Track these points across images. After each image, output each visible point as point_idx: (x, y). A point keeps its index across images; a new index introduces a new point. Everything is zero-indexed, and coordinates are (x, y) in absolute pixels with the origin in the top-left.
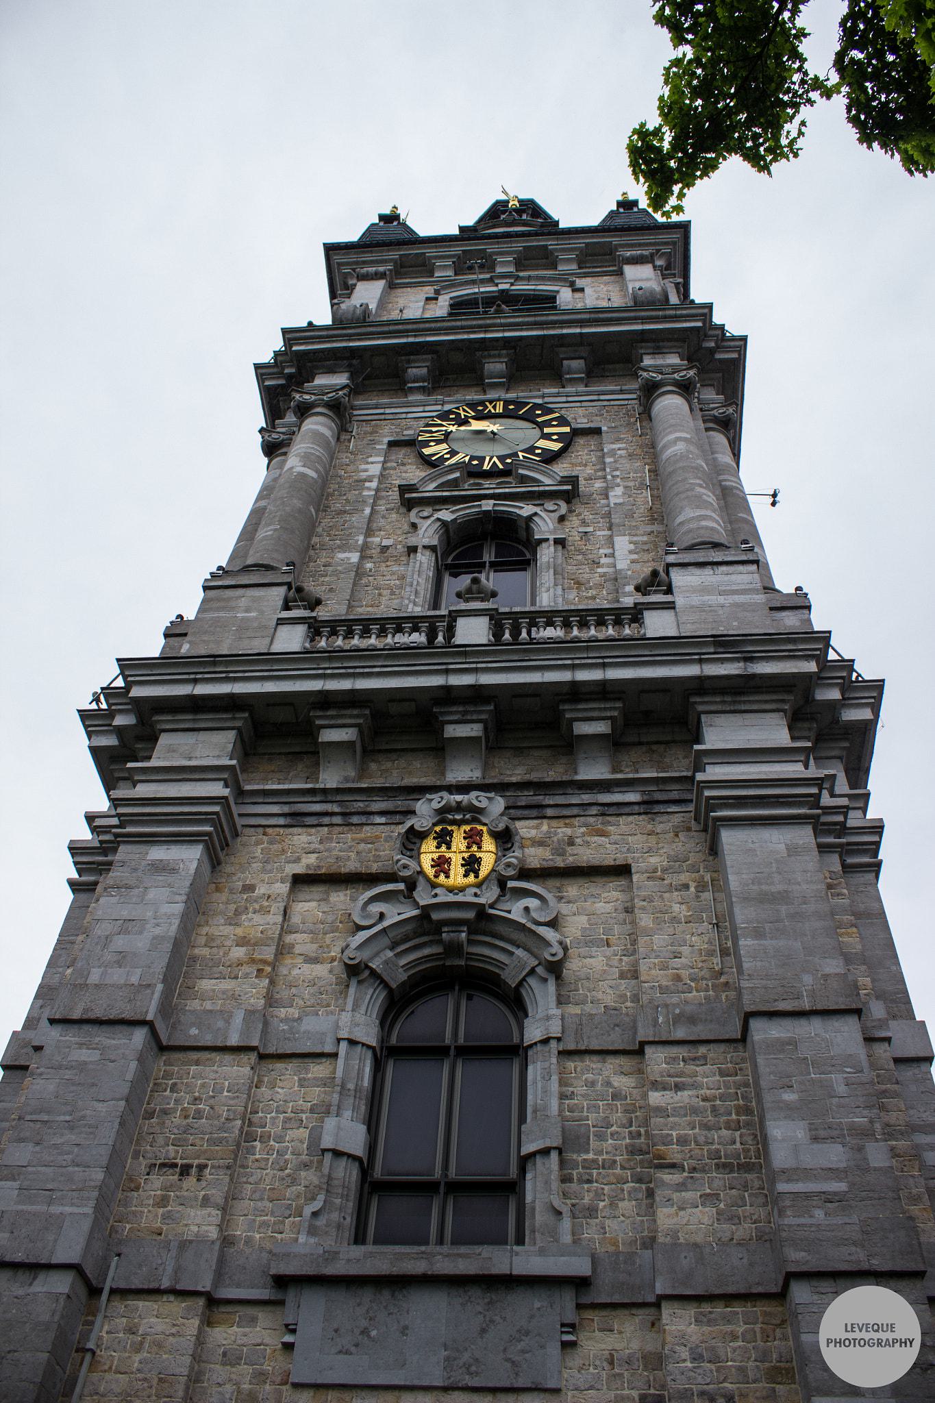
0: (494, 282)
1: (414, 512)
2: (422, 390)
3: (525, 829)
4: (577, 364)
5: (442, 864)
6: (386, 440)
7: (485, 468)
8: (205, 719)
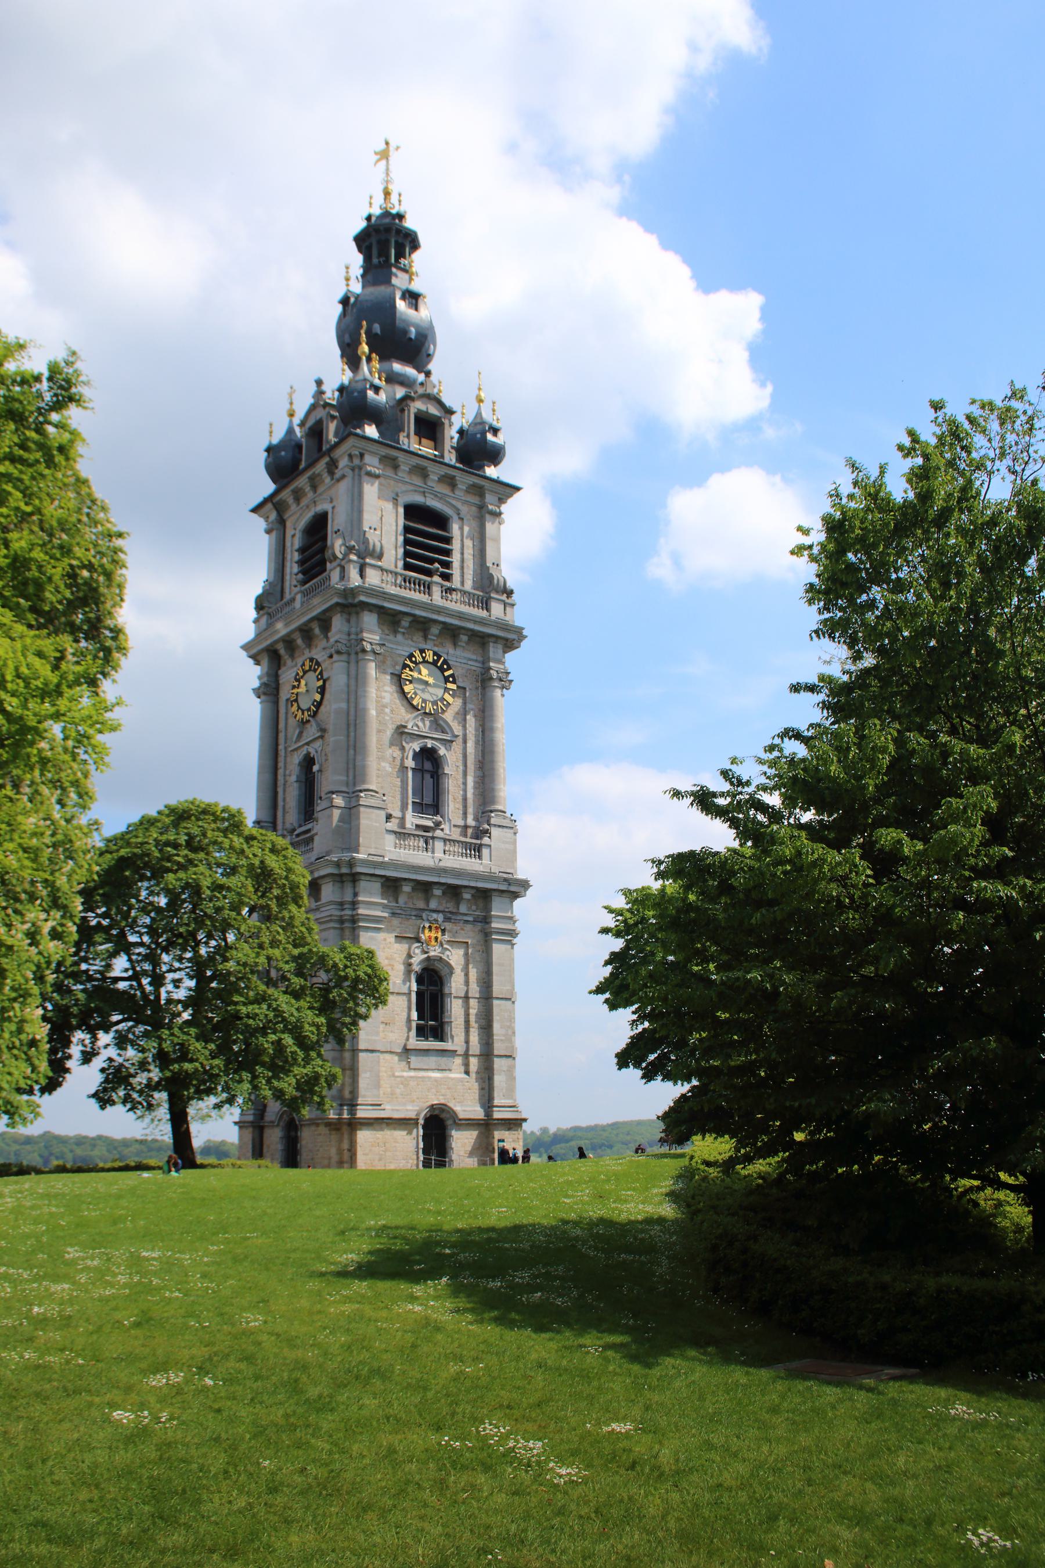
1: (404, 737)
2: (404, 633)
3: (448, 926)
5: (430, 937)
8: (374, 879)
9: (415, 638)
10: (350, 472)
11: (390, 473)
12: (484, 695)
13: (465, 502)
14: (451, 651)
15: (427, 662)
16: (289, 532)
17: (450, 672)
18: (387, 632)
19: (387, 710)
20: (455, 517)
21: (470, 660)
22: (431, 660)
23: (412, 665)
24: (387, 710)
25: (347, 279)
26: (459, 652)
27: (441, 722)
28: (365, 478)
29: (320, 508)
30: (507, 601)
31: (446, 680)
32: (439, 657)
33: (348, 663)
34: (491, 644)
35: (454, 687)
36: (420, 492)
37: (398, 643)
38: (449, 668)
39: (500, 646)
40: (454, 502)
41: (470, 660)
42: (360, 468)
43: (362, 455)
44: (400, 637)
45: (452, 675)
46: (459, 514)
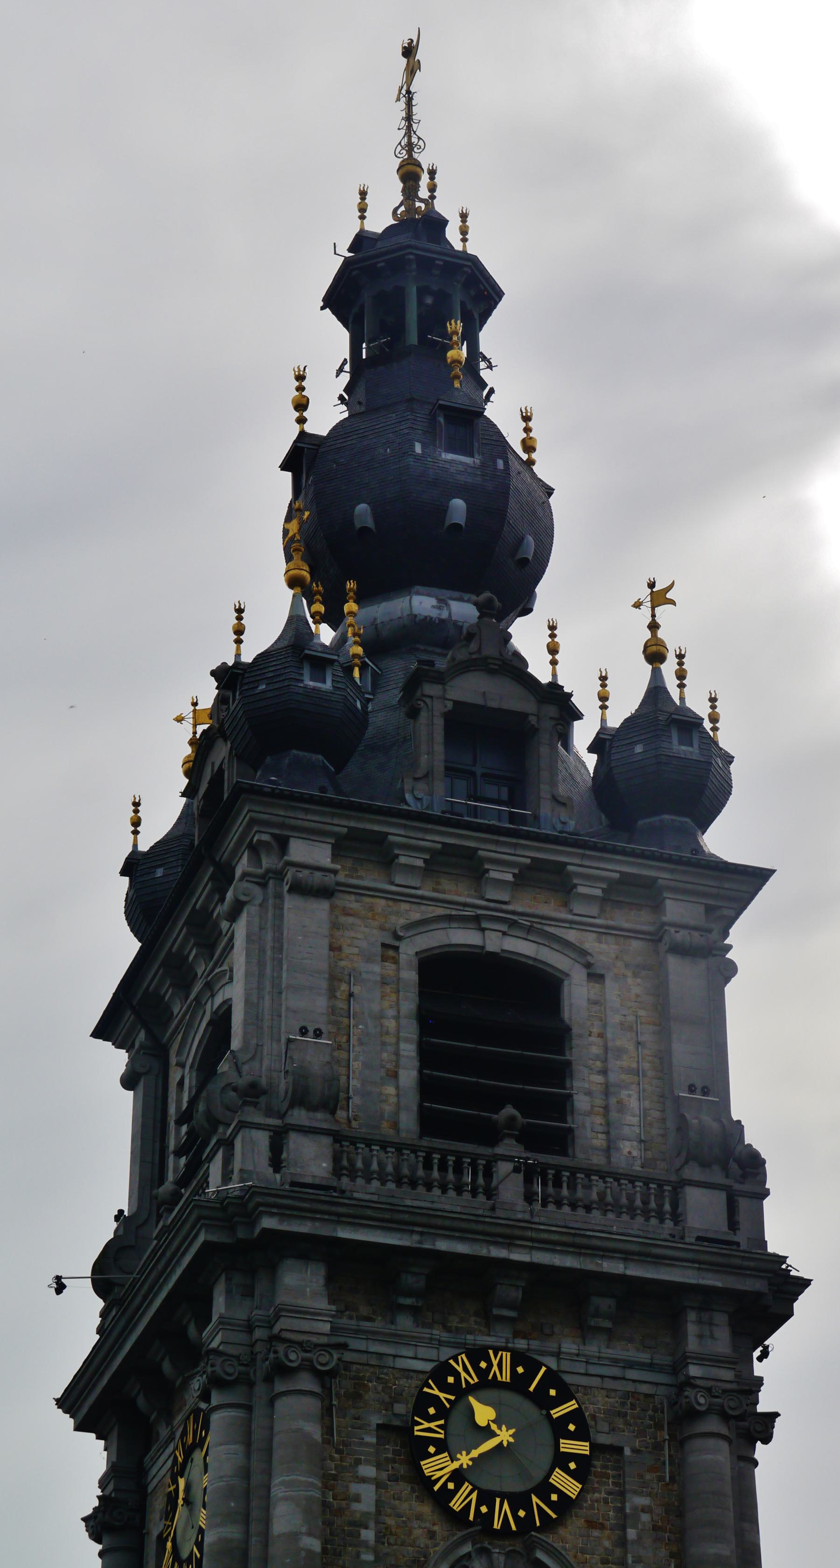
0: (479, 923)
2: (415, 1311)
4: (605, 1304)
6: (375, 1420)
7: (495, 1526)
9: (454, 1321)
10: (257, 890)
11: (370, 878)
12: (679, 1465)
13: (605, 932)
14: (569, 1346)
15: (496, 1384)
16: (175, 1075)
17: (571, 1406)
18: (364, 1310)
19: (368, 1535)
20: (578, 975)
21: (630, 1365)
22: (506, 1377)
23: (442, 1396)
24: (368, 1535)
25: (301, 405)
26: (592, 1348)
27: (540, 1555)
28: (291, 903)
29: (218, 1000)
30: (737, 1186)
31: (559, 1429)
32: (533, 1367)
33: (249, 1408)
34: (692, 1316)
35: (582, 1448)
37: (397, 1339)
38: (565, 1396)
39: (721, 1319)
40: (572, 936)
41: (630, 1365)
42: (279, 875)
43: (283, 844)
44: (405, 1323)
45: (575, 1416)
46: (588, 965)
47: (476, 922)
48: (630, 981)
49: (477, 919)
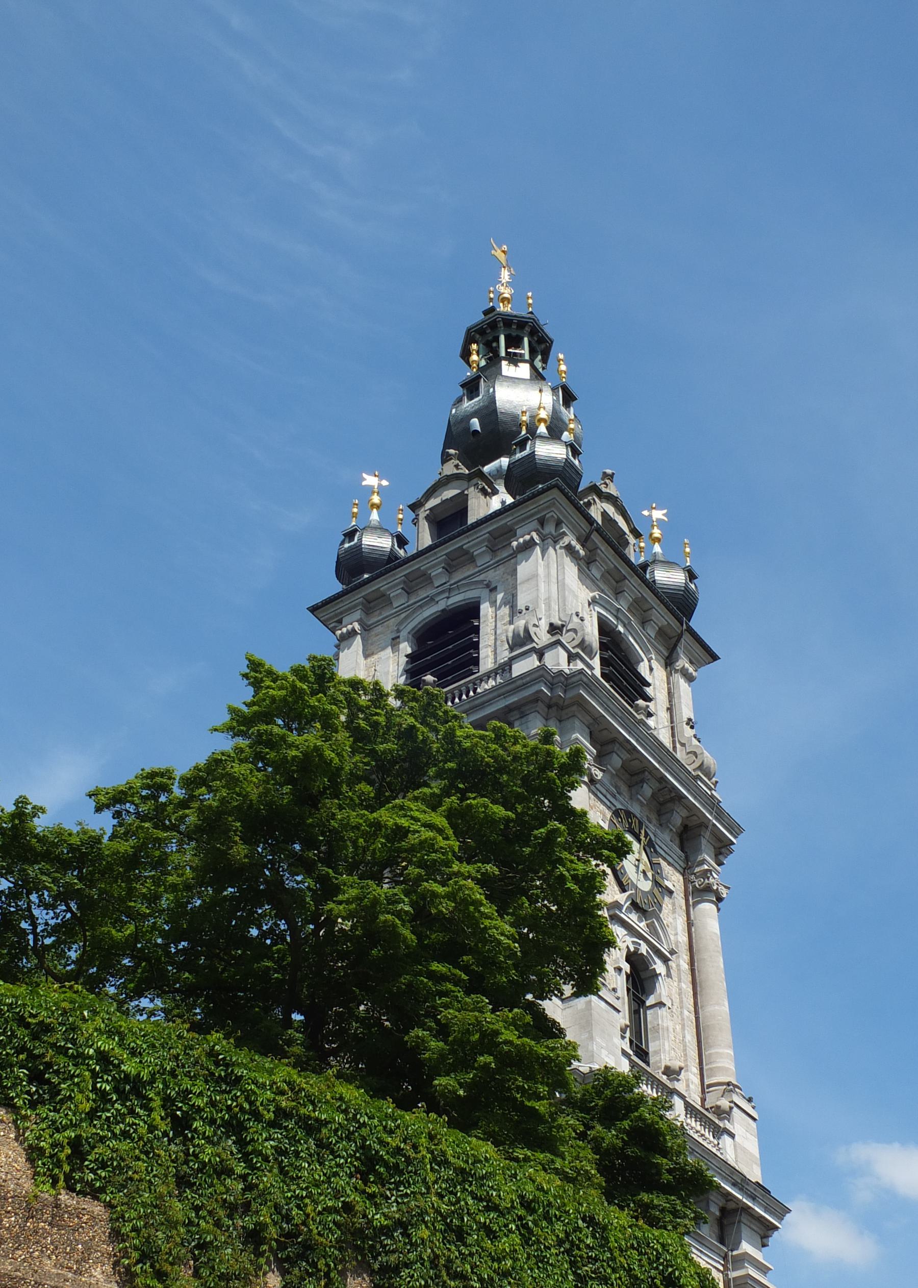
36: (426, 604)
47: (432, 600)
48: (509, 580)
49: (432, 599)
